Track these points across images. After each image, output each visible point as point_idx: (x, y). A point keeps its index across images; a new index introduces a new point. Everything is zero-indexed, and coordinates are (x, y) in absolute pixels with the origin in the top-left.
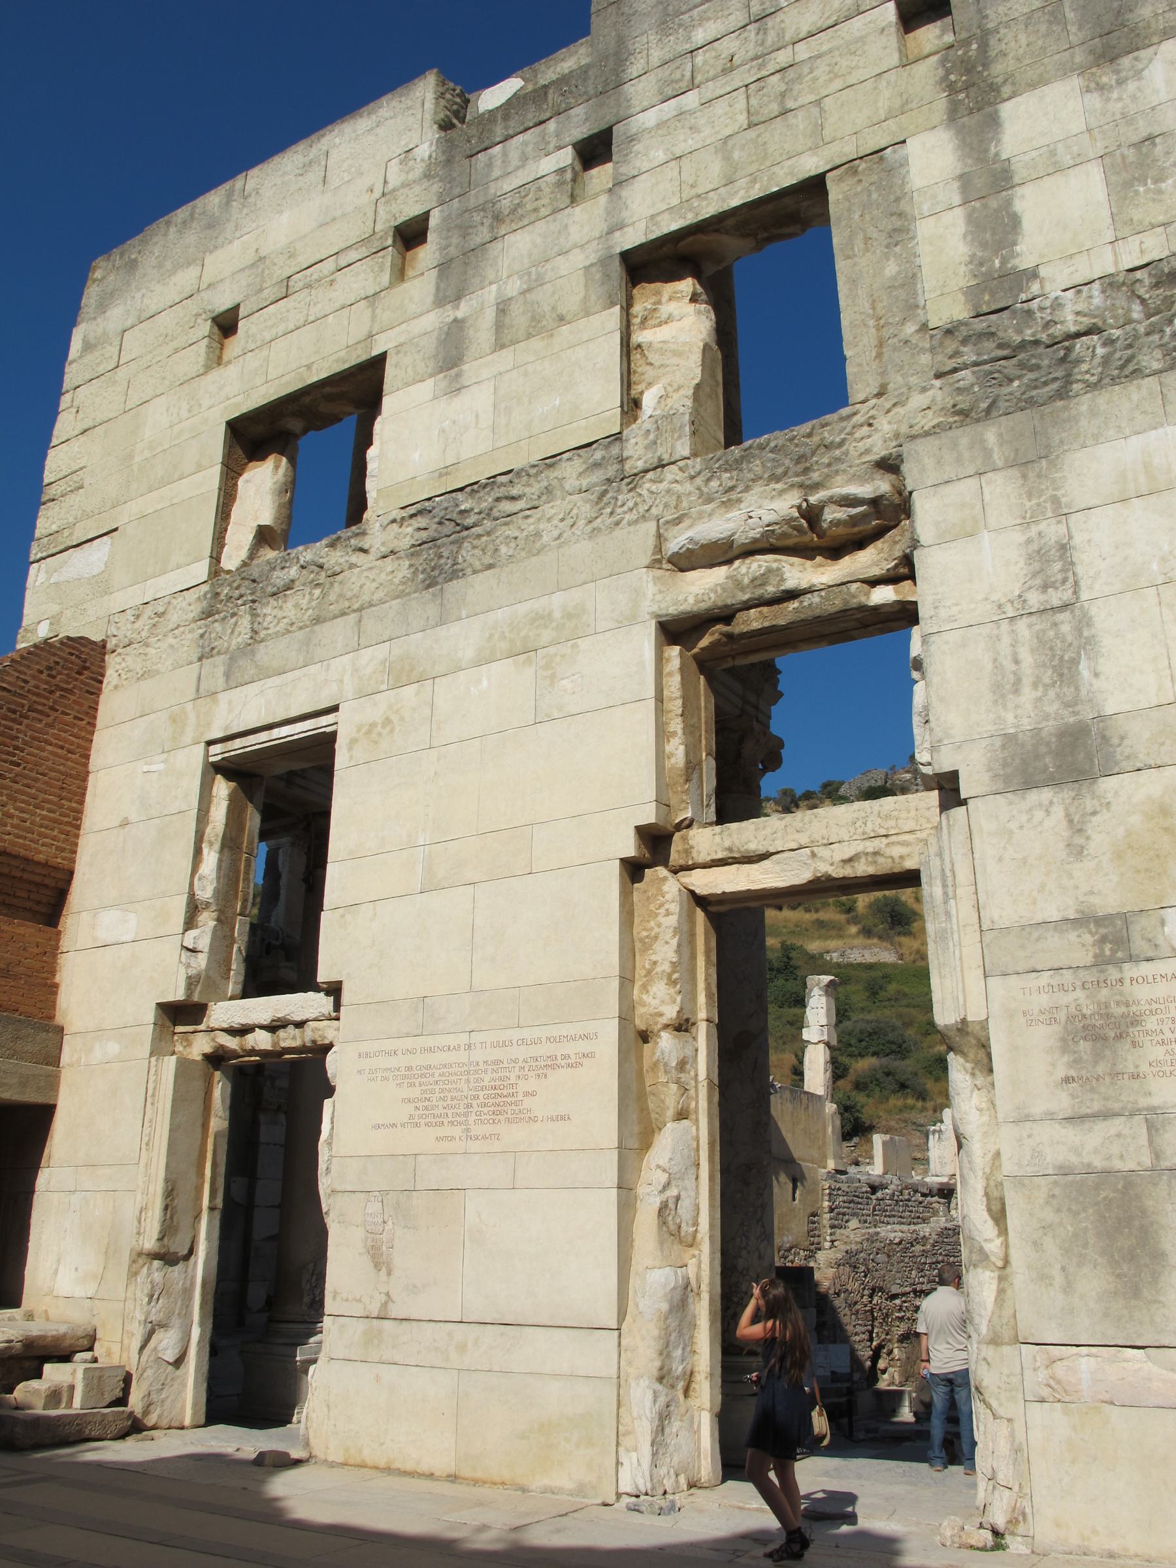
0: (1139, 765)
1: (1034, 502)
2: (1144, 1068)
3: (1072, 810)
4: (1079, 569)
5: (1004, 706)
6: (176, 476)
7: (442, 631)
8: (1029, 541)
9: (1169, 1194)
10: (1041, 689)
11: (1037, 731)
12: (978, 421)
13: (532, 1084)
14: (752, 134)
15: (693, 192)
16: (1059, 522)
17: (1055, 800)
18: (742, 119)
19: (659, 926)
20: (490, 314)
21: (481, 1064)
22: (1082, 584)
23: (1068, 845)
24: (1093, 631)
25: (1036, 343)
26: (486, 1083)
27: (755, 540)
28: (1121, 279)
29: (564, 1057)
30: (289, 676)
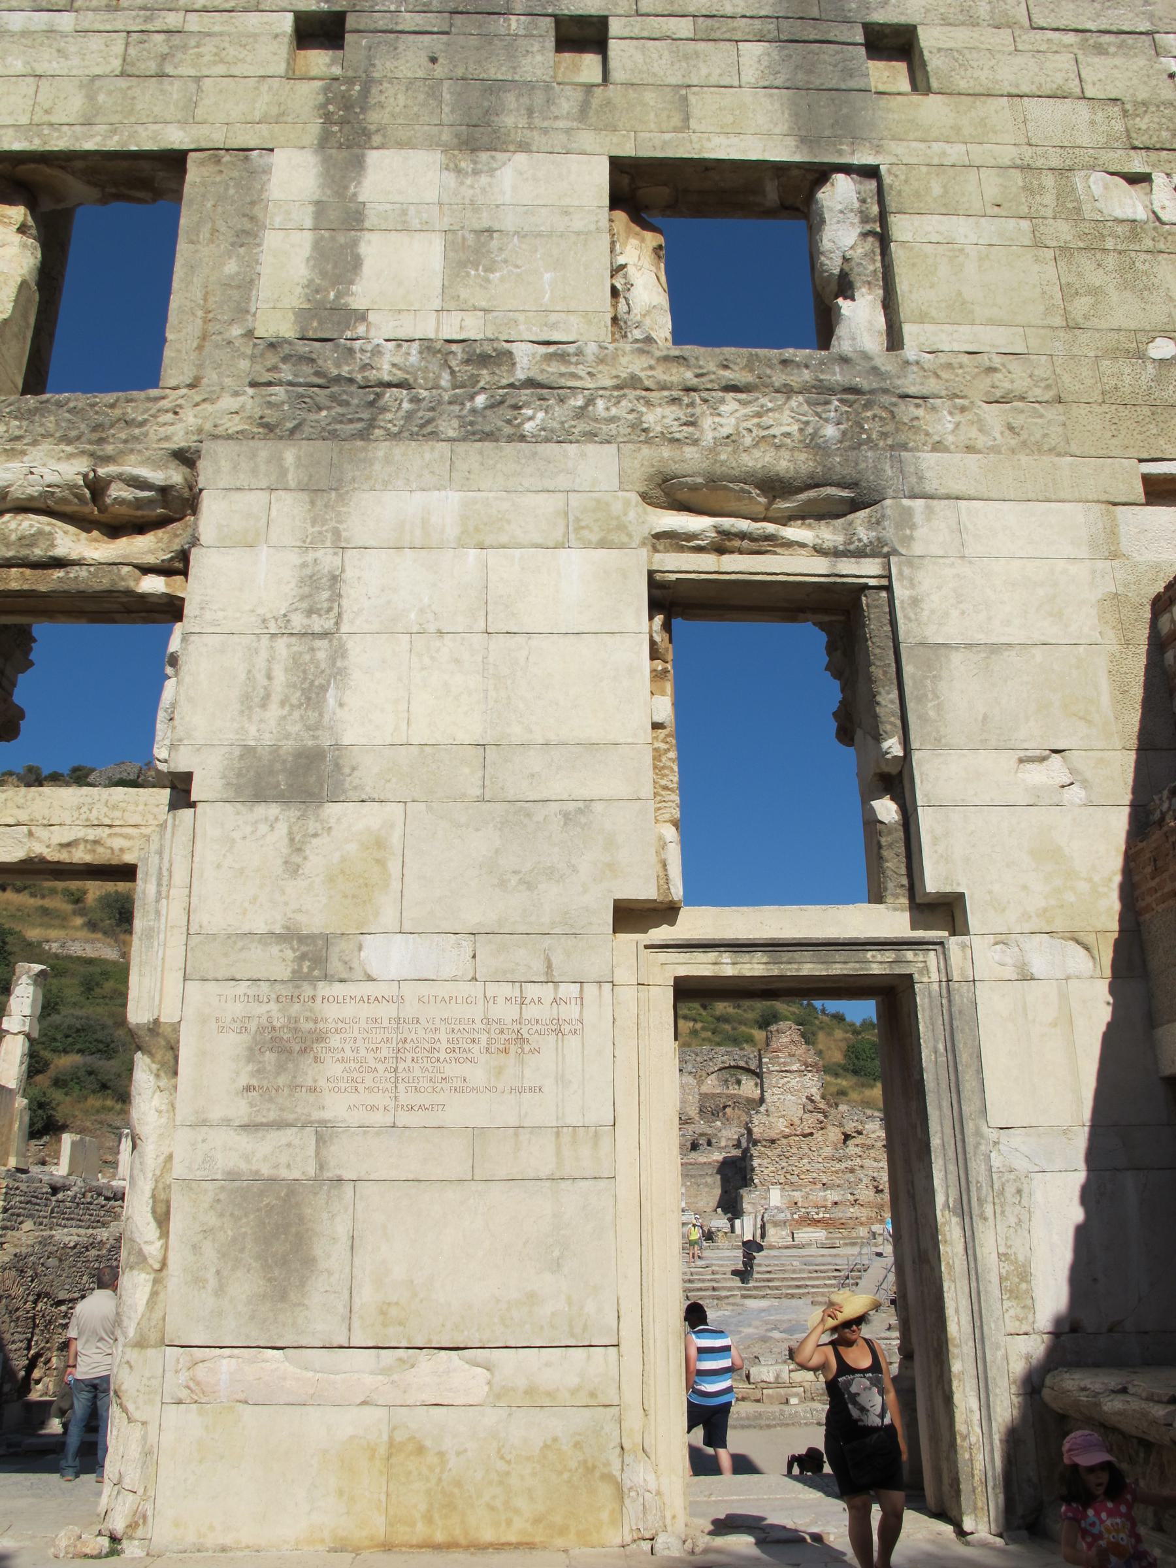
0: (364, 797)
1: (317, 529)
2: (322, 1083)
3: (295, 829)
4: (345, 603)
5: (250, 718)
8: (304, 565)
9: (327, 1203)
10: (287, 708)
11: (275, 749)
12: (281, 438)
14: (123, 83)
15: (46, 118)
16: (335, 554)
17: (281, 817)
18: (116, 64)
22: (345, 617)
23: (286, 862)
24: (346, 663)
25: (351, 381)
27: (31, 498)
28: (438, 345)
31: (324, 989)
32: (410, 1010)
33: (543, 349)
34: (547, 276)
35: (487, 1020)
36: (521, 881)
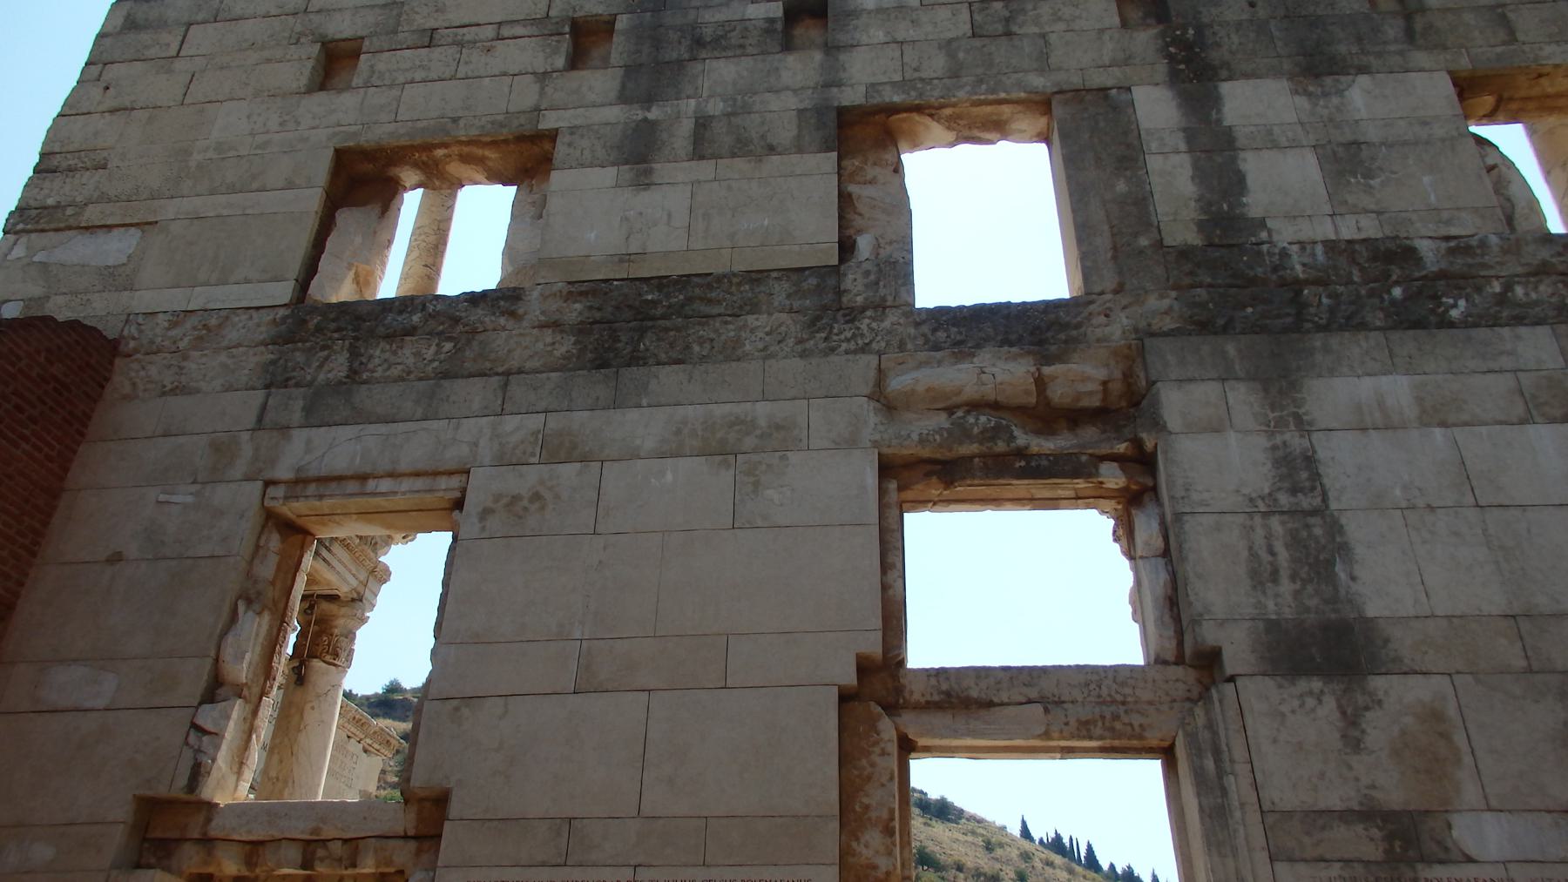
0: (1405, 669)
4: (1325, 481)
5: (1264, 593)
6: (255, 186)
7: (616, 415)
8: (1274, 448)
12: (1215, 333)
14: (977, 43)
15: (916, 75)
18: (967, 28)
19: (873, 765)
20: (687, 126)
30: (401, 427)
33: (1444, 245)
34: (1426, 179)
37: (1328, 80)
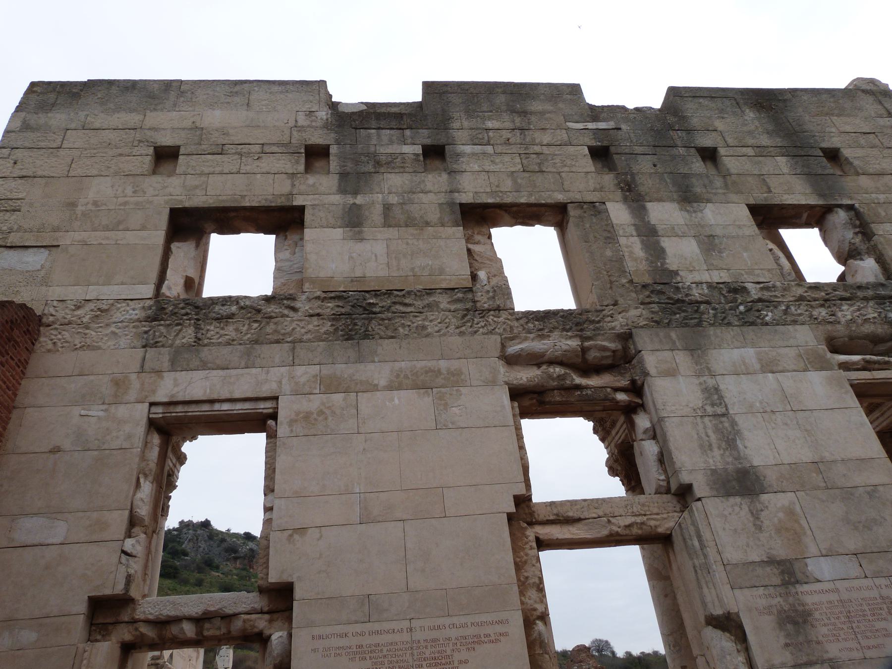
2: (820, 638)
4: (726, 400)
7: (361, 366)
8: (701, 384)
11: (726, 470)
13: (464, 655)
14: (527, 175)
15: (498, 189)
19: (527, 555)
20: (379, 209)
21: (422, 641)
25: (683, 301)
26: (427, 655)
27: (557, 357)
28: (715, 285)
29: (486, 636)
31: (801, 588)
32: (845, 596)
33: (758, 286)
34: (745, 254)
35: (882, 597)
36: (864, 526)
37: (695, 205)
